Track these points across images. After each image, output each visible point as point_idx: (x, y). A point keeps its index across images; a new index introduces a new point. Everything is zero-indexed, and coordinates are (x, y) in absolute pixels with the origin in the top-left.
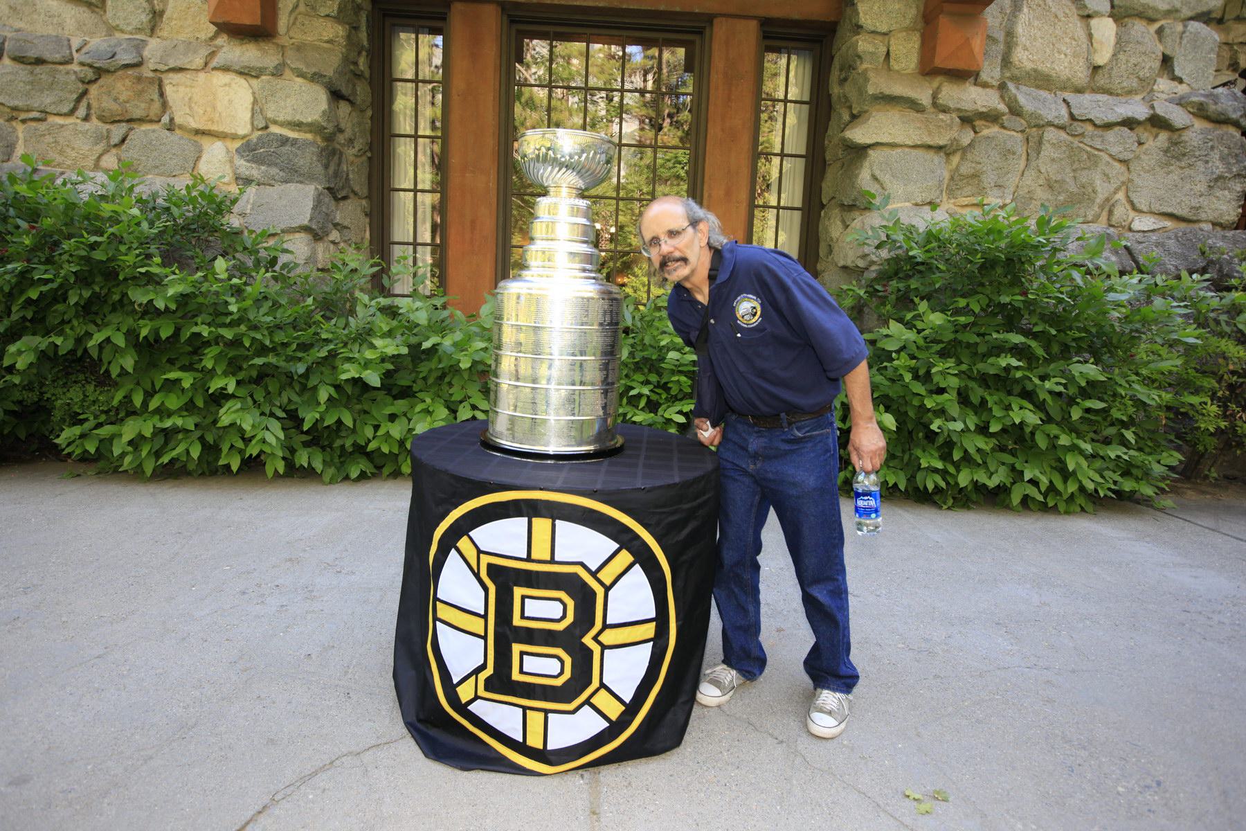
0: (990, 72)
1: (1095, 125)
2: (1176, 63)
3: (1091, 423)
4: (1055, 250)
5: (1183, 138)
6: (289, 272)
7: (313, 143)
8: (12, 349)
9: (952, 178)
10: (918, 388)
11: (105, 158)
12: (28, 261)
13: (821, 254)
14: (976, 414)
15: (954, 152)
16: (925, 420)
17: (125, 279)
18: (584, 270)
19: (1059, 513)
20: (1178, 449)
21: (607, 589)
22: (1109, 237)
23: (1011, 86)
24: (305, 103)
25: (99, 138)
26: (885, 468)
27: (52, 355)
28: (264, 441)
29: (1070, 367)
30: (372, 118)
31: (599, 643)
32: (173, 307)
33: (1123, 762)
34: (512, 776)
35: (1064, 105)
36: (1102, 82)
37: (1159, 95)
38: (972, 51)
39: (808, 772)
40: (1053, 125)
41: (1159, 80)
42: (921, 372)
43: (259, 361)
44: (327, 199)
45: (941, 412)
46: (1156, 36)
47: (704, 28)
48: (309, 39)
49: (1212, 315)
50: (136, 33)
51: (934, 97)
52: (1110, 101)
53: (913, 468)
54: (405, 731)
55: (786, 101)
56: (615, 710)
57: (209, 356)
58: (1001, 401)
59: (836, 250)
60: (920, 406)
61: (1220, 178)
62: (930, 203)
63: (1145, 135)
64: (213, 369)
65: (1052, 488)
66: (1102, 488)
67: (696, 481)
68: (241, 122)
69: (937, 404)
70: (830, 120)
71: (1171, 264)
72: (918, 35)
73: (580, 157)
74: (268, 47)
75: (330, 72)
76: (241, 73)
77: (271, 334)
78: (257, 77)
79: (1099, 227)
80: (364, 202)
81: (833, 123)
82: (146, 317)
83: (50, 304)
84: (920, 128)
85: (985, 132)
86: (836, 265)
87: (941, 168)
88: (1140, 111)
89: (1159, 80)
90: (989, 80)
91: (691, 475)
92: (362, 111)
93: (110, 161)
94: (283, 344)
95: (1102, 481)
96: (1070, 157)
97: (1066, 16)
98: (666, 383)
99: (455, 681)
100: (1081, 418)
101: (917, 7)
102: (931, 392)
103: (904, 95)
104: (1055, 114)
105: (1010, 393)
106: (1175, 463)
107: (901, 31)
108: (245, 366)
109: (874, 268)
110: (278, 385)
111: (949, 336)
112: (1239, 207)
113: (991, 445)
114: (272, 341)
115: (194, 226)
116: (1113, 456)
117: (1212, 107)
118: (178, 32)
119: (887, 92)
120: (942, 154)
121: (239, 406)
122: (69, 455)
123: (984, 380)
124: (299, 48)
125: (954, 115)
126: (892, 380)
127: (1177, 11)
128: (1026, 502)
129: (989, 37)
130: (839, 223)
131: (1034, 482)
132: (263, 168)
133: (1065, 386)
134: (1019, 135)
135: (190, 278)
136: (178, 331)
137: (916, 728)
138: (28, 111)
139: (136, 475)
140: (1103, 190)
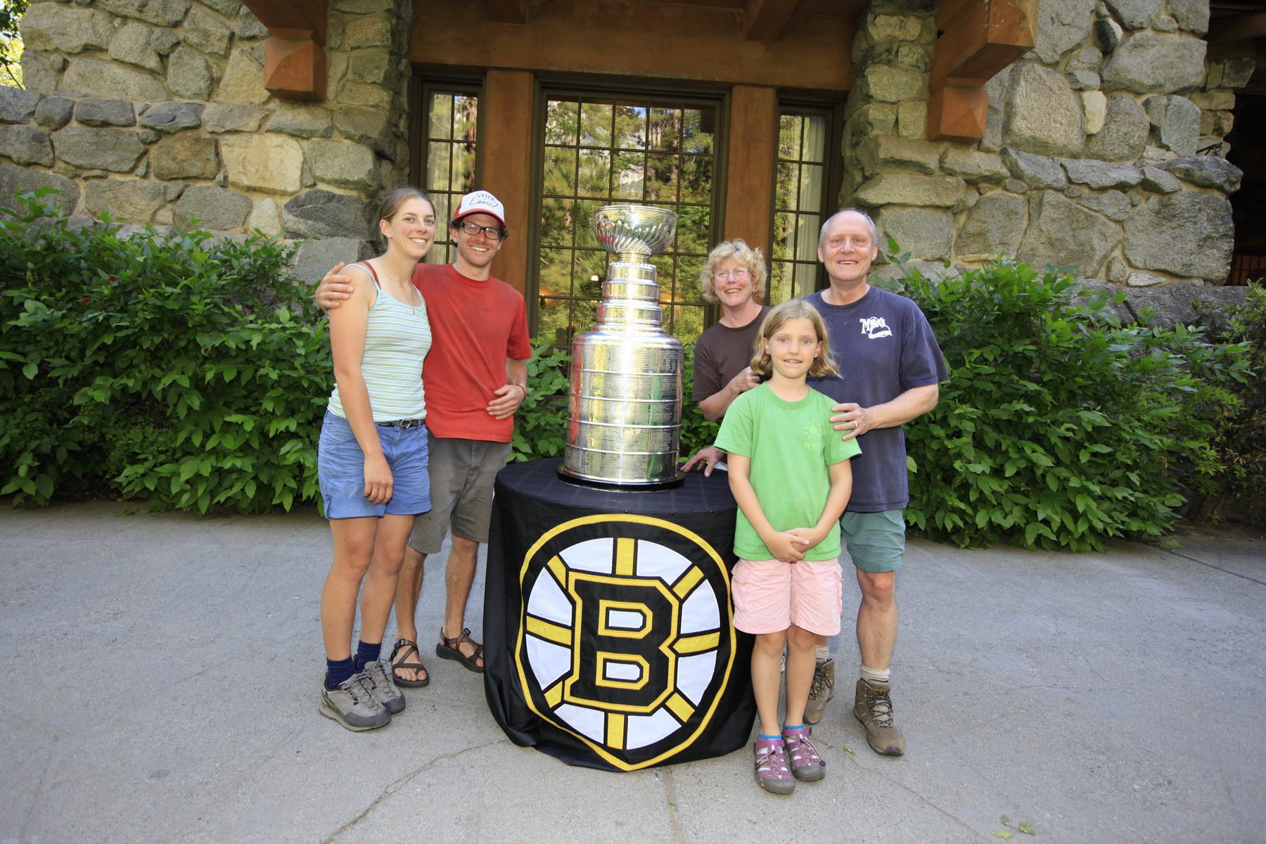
0: (993, 139)
1: (1091, 188)
2: (1162, 133)
3: (1099, 466)
5: (1172, 201)
7: (358, 200)
9: (959, 236)
11: (161, 212)
12: (105, 309)
14: (990, 457)
15: (961, 212)
16: (944, 461)
17: (194, 327)
18: (656, 326)
20: (1182, 492)
21: (681, 601)
23: (1012, 152)
24: (352, 163)
25: (156, 194)
30: (409, 176)
31: (674, 651)
35: (1061, 169)
36: (1096, 149)
38: (975, 121)
39: (858, 772)
40: (1052, 188)
41: (1148, 147)
46: (1143, 108)
47: (724, 95)
48: (355, 103)
49: (1208, 364)
50: (194, 98)
51: (941, 161)
55: (800, 162)
56: (686, 713)
61: (1208, 238)
62: (941, 259)
63: (1137, 199)
64: (273, 413)
65: (1063, 527)
70: (842, 180)
71: (1167, 317)
72: (924, 104)
74: (319, 112)
75: (375, 134)
76: (292, 135)
77: (326, 378)
78: (308, 139)
79: (1099, 282)
81: (846, 184)
85: (989, 194)
87: (949, 227)
88: (1132, 176)
89: (1148, 147)
90: (991, 146)
92: (401, 169)
93: (166, 215)
95: (1110, 521)
96: (1069, 217)
97: (1060, 89)
98: (696, 428)
99: (543, 688)
101: (923, 80)
102: (949, 437)
105: (1021, 438)
107: (909, 100)
108: (303, 409)
112: (1228, 264)
113: (1005, 487)
116: (1120, 498)
117: (1198, 173)
118: (233, 97)
119: (898, 157)
123: (997, 425)
124: (347, 112)
125: (960, 178)
127: (1161, 86)
128: (1039, 542)
129: (990, 107)
131: (1046, 522)
132: (310, 222)
134: (1021, 197)
136: (239, 373)
138: (91, 169)
139: (192, 513)
140: (1100, 248)
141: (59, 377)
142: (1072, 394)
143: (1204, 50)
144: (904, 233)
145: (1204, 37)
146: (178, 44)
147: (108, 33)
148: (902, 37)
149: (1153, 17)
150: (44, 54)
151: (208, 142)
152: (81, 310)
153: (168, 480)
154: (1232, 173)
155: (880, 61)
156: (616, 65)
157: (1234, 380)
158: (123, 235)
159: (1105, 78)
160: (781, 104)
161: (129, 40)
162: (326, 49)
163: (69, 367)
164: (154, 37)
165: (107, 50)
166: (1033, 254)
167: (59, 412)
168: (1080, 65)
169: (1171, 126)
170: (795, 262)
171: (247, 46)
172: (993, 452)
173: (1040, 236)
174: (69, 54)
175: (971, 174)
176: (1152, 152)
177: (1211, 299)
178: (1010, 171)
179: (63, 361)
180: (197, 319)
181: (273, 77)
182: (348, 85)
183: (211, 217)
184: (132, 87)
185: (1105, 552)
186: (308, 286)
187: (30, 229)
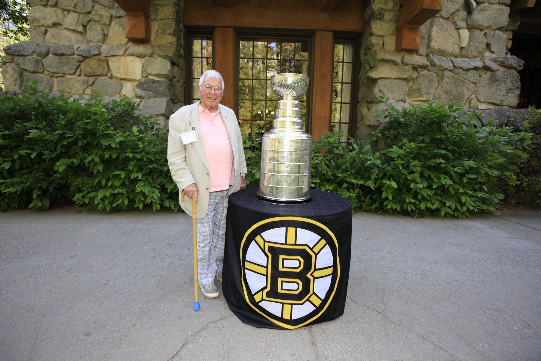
0: (423, 50)
2: (491, 46)
4: (455, 118)
5: (496, 74)
6: (158, 132)
7: (165, 82)
8: (58, 164)
9: (409, 91)
10: (405, 172)
12: (63, 130)
13: (358, 120)
15: (410, 80)
16: (407, 183)
17: (99, 136)
18: (300, 129)
22: (470, 111)
23: (431, 55)
27: (71, 165)
28: (152, 197)
29: (463, 162)
30: (185, 72)
32: (118, 146)
38: (416, 43)
40: (448, 70)
43: (150, 166)
44: (171, 103)
45: (413, 181)
51: (402, 60)
52: (468, 61)
58: (436, 176)
59: (365, 119)
61: (510, 89)
62: (402, 100)
63: (482, 73)
64: (133, 170)
65: (456, 209)
69: (412, 178)
72: (395, 36)
74: (148, 46)
75: (171, 55)
76: (138, 56)
77: (154, 156)
78: (144, 58)
81: (362, 70)
85: (422, 73)
86: (365, 124)
87: (405, 87)
88: (480, 64)
90: (422, 53)
92: (182, 69)
94: (160, 160)
95: (475, 205)
96: (454, 82)
97: (450, 28)
100: (467, 182)
101: (394, 26)
103: (391, 59)
104: (449, 65)
105: (439, 173)
108: (145, 168)
109: (382, 125)
111: (415, 151)
113: (433, 193)
114: (155, 159)
116: (479, 196)
117: (506, 62)
119: (385, 58)
120: (406, 81)
121: (143, 184)
122: (76, 204)
123: (429, 168)
124: (159, 46)
125: (410, 66)
126: (393, 168)
127: (491, 27)
129: (422, 37)
130: (366, 108)
131: (450, 207)
132: (146, 92)
134: (435, 74)
135: (125, 135)
139: (104, 211)
140: (467, 94)
142: (460, 154)
143: (508, 11)
144: (387, 90)
145: (509, 6)
148: (385, 8)
151: (104, 60)
152: (55, 130)
154: (520, 62)
155: (377, 19)
156: (268, 24)
157: (523, 147)
163: (52, 154)
167: (50, 172)
168: (458, 18)
169: (495, 43)
170: (341, 103)
172: (429, 179)
173: (442, 90)
176: (487, 54)
177: (512, 114)
178: (430, 63)
179: (49, 152)
181: (128, 33)
182: (159, 35)
186: (146, 118)
187: (33, 98)
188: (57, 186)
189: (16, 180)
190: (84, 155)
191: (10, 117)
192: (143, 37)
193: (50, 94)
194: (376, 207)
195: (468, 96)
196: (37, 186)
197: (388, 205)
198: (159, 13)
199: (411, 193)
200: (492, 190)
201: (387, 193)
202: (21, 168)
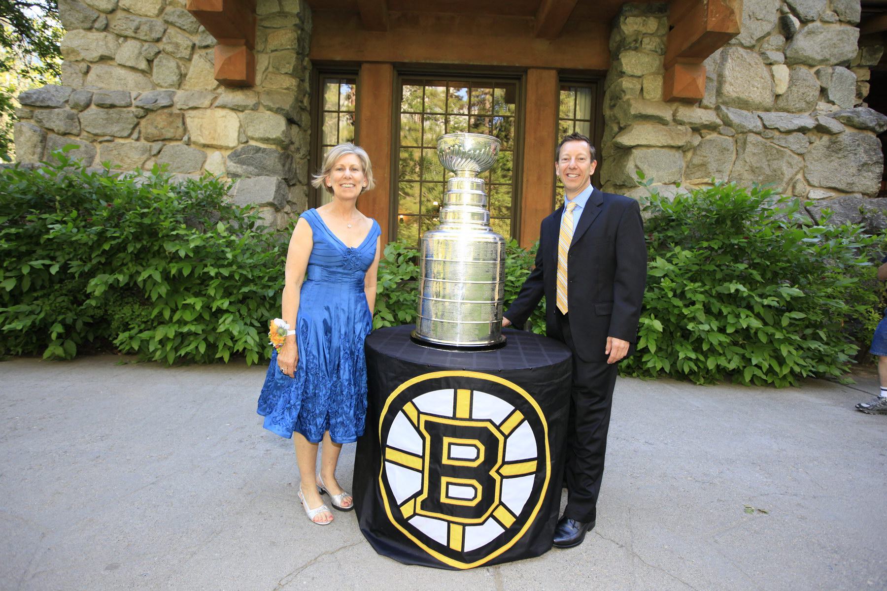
0: (709, 99)
1: (780, 132)
2: (829, 92)
5: (839, 139)
6: (261, 232)
7: (275, 151)
8: (93, 282)
9: (688, 167)
10: (678, 302)
11: (148, 163)
14: (717, 320)
15: (689, 150)
16: (682, 324)
17: (163, 237)
19: (775, 387)
20: (852, 342)
23: (723, 108)
25: (145, 151)
26: (656, 357)
27: (116, 286)
28: (246, 342)
30: (310, 135)
32: (191, 255)
33: (866, 563)
34: (440, 570)
35: (758, 119)
36: (782, 105)
37: (821, 112)
38: (697, 87)
39: (645, 568)
40: (753, 132)
42: (678, 292)
43: (245, 290)
44: (284, 186)
46: (815, 76)
47: (522, 76)
51: (674, 115)
53: (672, 356)
54: (362, 537)
57: (213, 286)
58: (733, 311)
60: (678, 315)
62: (674, 183)
63: (813, 138)
65: (770, 370)
66: (805, 370)
67: (563, 363)
68: (231, 138)
69: (691, 312)
70: (603, 131)
73: (481, 151)
74: (250, 93)
75: (287, 107)
76: (232, 109)
77: (251, 271)
78: (242, 111)
80: (305, 188)
82: (174, 261)
83: (115, 254)
84: (665, 135)
87: (678, 160)
88: (810, 123)
89: (819, 103)
90: (709, 104)
91: (559, 360)
92: (305, 131)
96: (765, 152)
97: (756, 64)
98: (507, 301)
99: (399, 503)
100: (790, 323)
102: (686, 306)
104: (754, 125)
105: (739, 306)
106: (855, 353)
107: (650, 74)
108: (235, 292)
110: (256, 304)
111: (696, 268)
112: (879, 183)
114: (252, 276)
115: (205, 203)
118: (195, 86)
119: (644, 113)
121: (231, 318)
122: (120, 351)
123: (720, 297)
124: (268, 93)
125: (688, 127)
127: (827, 60)
129: (707, 78)
132: (244, 167)
133: (778, 302)
134: (731, 139)
137: (713, 537)
138: (104, 136)
139: (163, 363)
140: (788, 173)
141: (75, 273)
142: (775, 274)
143: (857, 35)
144: (649, 166)
145: (857, 26)
146: (159, 52)
147: (115, 47)
148: (645, 31)
149: (821, 12)
150: (76, 63)
151: (178, 115)
153: (145, 343)
155: (630, 48)
156: (449, 57)
158: (121, 178)
159: (788, 55)
160: (561, 81)
161: (128, 52)
162: (254, 52)
163: (85, 265)
164: (144, 48)
165: (114, 59)
166: (740, 179)
167: (79, 296)
168: (770, 47)
171: (203, 52)
172: (719, 315)
173: (745, 165)
174: (91, 62)
175: (695, 124)
176: (822, 106)
179: (79, 263)
180: (164, 231)
182: (269, 76)
183: (179, 165)
184: (130, 82)
185: (800, 387)
187: (60, 174)
188: (90, 321)
189: (23, 307)
190: (135, 268)
191: (19, 205)
192: (242, 79)
193: (88, 169)
194: (629, 363)
195: (790, 176)
196: (56, 319)
197: (649, 361)
198: (269, 40)
199: (690, 341)
200: (837, 338)
201: (647, 340)
202: (33, 288)
